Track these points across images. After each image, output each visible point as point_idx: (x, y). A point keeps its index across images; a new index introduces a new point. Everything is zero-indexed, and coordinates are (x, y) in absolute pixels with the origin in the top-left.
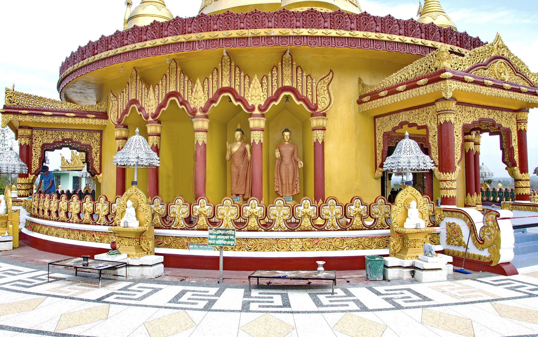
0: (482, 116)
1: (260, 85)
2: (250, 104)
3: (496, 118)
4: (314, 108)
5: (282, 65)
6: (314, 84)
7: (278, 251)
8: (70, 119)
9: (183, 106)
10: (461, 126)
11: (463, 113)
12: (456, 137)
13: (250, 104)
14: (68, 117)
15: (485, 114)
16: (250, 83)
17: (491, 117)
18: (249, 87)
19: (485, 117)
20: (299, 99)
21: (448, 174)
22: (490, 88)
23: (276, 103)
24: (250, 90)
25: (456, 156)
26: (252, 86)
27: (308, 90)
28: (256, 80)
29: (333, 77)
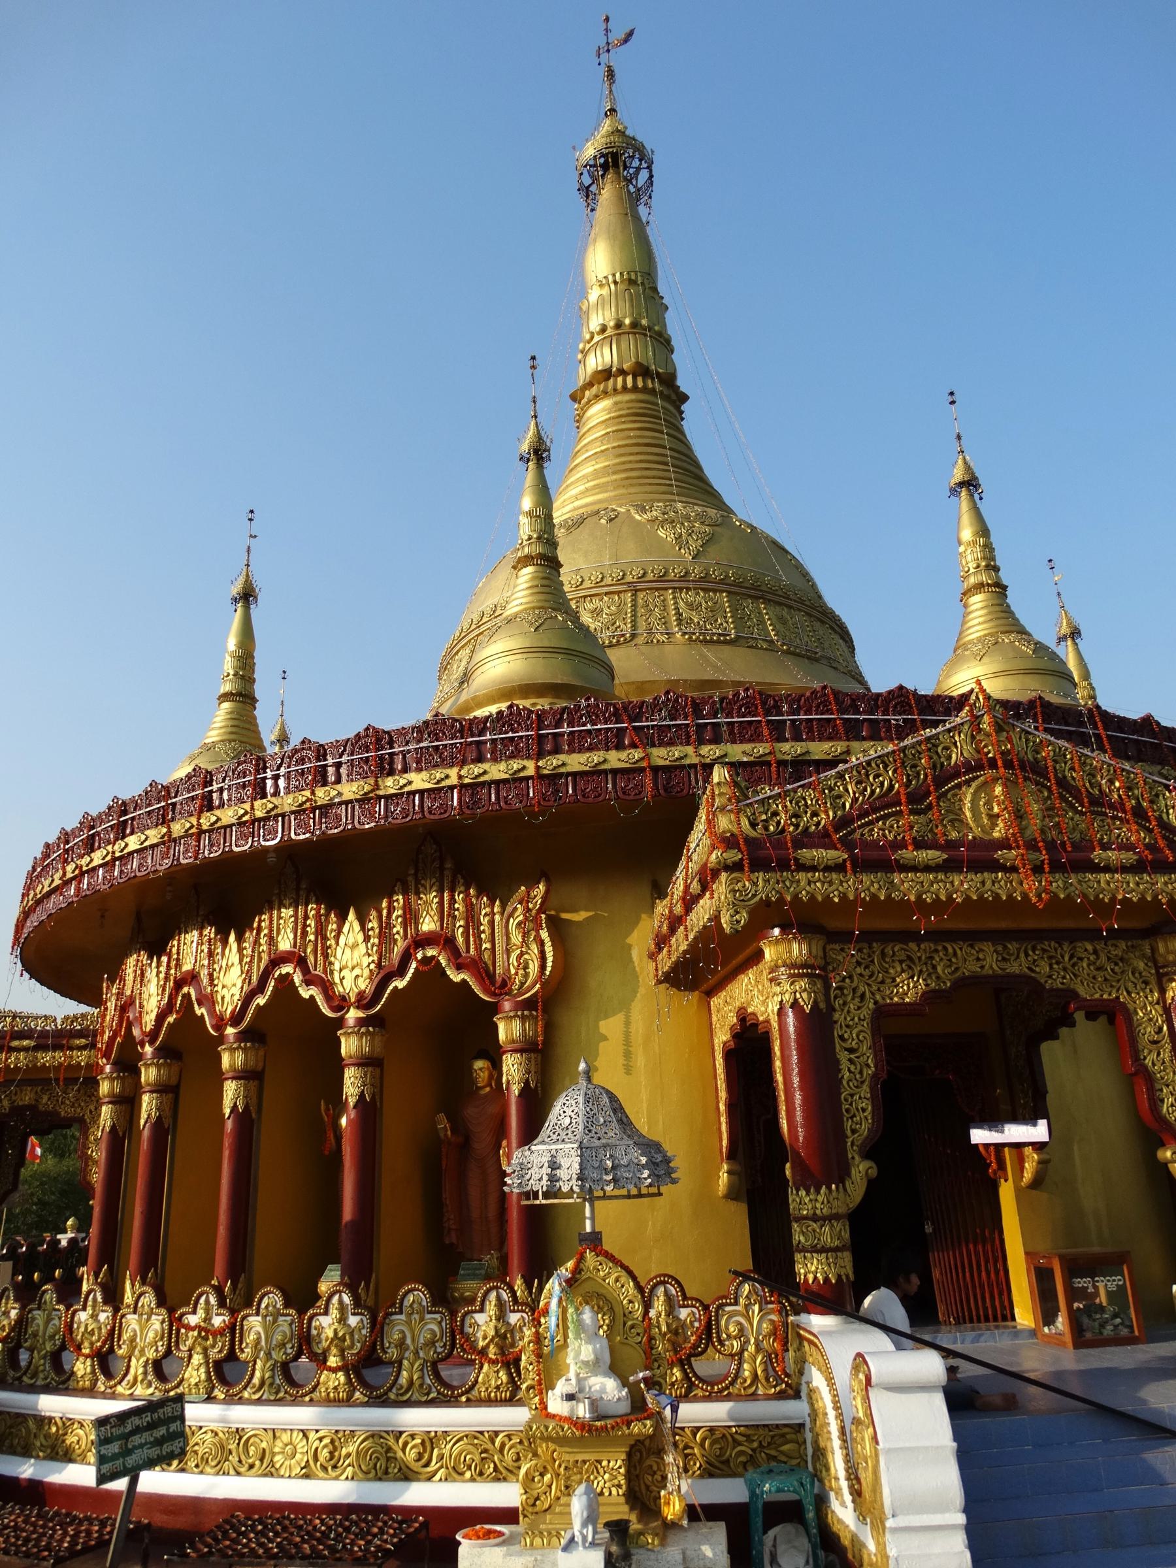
0: (971, 967)
1: (360, 937)
2: (339, 989)
3: (1044, 968)
4: (504, 988)
5: (416, 874)
6: (497, 918)
7: (238, 1473)
8: (22, 1055)
9: (203, 1010)
10: (865, 1012)
11: (876, 967)
12: (843, 1056)
13: (339, 989)
14: (18, 1050)
15: (987, 960)
16: (339, 932)
17: (1014, 968)
18: (337, 944)
19: (987, 971)
20: (459, 968)
21: (803, 1193)
22: (941, 876)
23: (400, 984)
24: (339, 951)
25: (849, 1124)
26: (342, 939)
27: (483, 936)
28: (351, 926)
29: (547, 892)
